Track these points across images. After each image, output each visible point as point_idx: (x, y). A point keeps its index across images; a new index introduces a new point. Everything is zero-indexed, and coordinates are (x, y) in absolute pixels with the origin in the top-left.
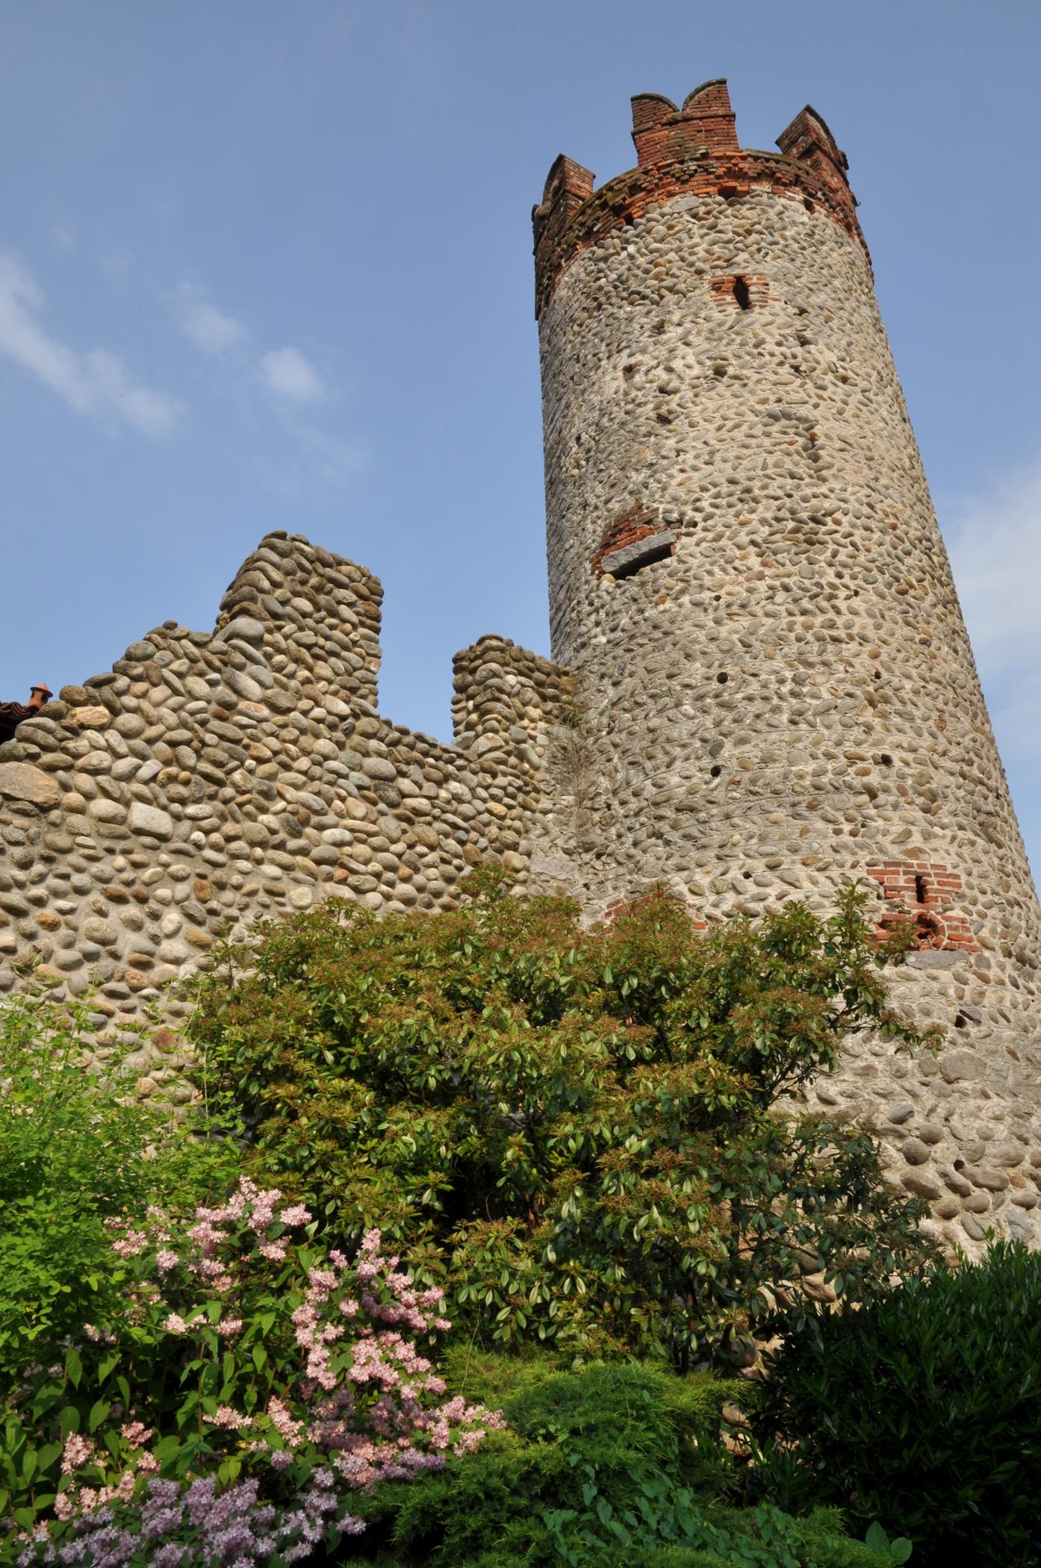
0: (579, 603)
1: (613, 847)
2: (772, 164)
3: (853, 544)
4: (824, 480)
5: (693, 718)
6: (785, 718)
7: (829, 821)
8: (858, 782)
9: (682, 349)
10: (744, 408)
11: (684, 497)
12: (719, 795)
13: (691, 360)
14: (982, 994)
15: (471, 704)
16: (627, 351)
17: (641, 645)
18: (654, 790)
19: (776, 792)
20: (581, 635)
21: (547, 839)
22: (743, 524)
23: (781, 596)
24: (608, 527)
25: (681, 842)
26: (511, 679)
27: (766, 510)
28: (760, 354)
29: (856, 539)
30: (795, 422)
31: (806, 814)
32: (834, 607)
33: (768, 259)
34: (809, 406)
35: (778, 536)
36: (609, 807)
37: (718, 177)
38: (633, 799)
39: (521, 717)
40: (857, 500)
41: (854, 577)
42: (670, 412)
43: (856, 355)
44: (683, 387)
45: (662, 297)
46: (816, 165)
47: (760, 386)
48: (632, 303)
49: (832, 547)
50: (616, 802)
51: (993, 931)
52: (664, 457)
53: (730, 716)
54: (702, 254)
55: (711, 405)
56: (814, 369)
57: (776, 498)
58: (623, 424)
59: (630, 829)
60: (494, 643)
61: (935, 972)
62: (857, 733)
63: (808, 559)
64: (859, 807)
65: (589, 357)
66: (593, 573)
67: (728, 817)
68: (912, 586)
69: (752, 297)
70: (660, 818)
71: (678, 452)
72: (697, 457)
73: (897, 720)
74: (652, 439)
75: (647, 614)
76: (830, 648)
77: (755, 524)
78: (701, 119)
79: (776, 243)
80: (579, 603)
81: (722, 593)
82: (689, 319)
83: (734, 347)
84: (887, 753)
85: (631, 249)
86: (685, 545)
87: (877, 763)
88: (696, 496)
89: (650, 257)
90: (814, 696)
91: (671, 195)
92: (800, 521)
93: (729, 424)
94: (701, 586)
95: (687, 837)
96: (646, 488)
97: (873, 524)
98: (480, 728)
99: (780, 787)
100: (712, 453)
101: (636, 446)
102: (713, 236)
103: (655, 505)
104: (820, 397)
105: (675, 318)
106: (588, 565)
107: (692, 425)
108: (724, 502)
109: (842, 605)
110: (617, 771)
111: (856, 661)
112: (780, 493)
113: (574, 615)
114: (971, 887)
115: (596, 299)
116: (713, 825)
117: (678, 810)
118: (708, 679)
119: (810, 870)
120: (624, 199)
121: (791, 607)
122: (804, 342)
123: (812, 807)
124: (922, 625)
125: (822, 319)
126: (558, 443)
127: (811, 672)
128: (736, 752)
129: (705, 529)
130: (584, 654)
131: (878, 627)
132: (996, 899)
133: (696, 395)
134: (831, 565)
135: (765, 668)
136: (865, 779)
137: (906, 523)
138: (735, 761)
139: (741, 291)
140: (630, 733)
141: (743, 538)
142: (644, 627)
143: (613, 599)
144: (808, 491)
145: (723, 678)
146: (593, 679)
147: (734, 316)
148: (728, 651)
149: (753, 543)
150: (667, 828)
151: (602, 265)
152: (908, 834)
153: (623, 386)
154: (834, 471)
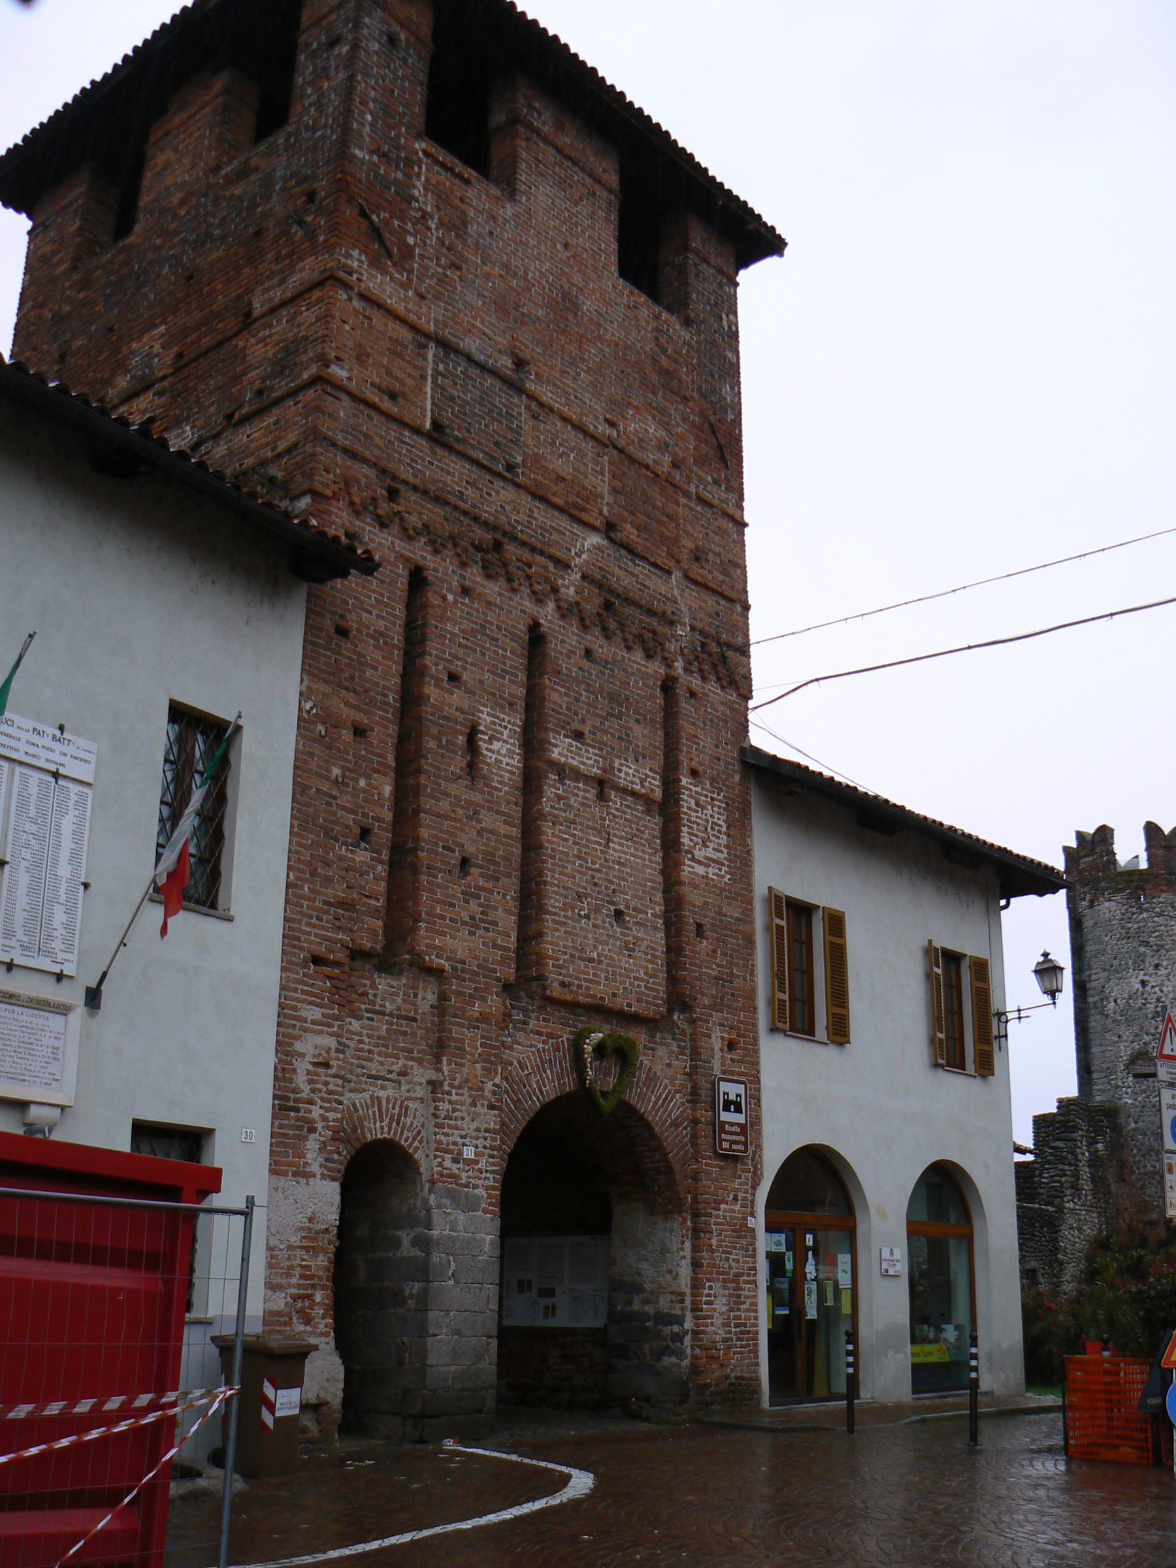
0: (1116, 1079)
9: (1166, 983)
13: (1170, 989)
16: (1142, 972)
91: (1163, 891)
153: (1141, 989)
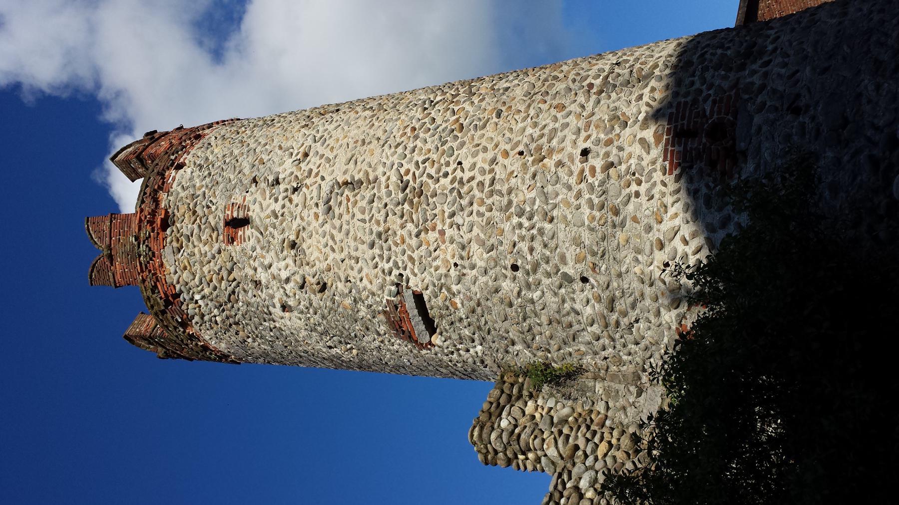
1: (638, 359)
2: (148, 190)
3: (424, 162)
4: (376, 179)
5: (543, 292)
6: (547, 226)
7: (629, 201)
8: (600, 176)
9: (274, 269)
10: (320, 231)
11: (380, 280)
12: (603, 279)
14: (774, 91)
15: (521, 457)
16: (271, 308)
17: (486, 323)
18: (595, 326)
19: (604, 238)
20: (474, 363)
21: (629, 409)
22: (403, 242)
23: (458, 219)
24: (397, 335)
25: (637, 311)
26: (504, 423)
27: (394, 222)
28: (282, 215)
29: (420, 159)
30: (333, 195)
31: (622, 217)
32: (469, 181)
33: (214, 201)
34: (323, 184)
35: (414, 217)
36: (605, 358)
37: (153, 230)
38: (601, 341)
39: (533, 417)
40: (392, 155)
41: (448, 164)
42: (318, 283)
43: (289, 144)
44: (301, 272)
45: (235, 280)
46: (153, 157)
47: (305, 218)
48: (237, 301)
49: (425, 178)
50: (603, 353)
51: (725, 78)
52: (350, 292)
53: (544, 266)
54: (207, 248)
55: (316, 254)
56: (297, 176)
57: (387, 215)
58: (323, 317)
59: (624, 346)
60: (476, 433)
61: (754, 129)
62: (562, 172)
63: (432, 197)
64: (620, 177)
65: (272, 334)
66: (430, 349)
67: (620, 275)
68: (457, 120)
69: (241, 216)
70: (618, 324)
71: (347, 281)
72: (352, 269)
73: (554, 142)
74: (336, 298)
75: (464, 316)
76: (497, 187)
77: (404, 232)
78: (111, 238)
79: (204, 193)
80: (451, 361)
81: (452, 262)
82: (252, 262)
83: (276, 233)
84: (579, 152)
85: (197, 297)
86: (415, 283)
87: (587, 160)
88: (380, 273)
89: (205, 284)
90: (534, 203)
91: (162, 265)
92: (405, 200)
93: (331, 243)
94: (446, 276)
95: (633, 306)
96: (371, 306)
97: (411, 145)
98: (539, 453)
99: (600, 235)
100: (350, 257)
101: (340, 310)
102: (194, 239)
103: (384, 301)
104: (317, 174)
105: (251, 272)
106: (424, 352)
107: (329, 270)
108: (386, 253)
109: (467, 175)
110: (579, 350)
111: (509, 169)
112: (383, 212)
113: (459, 365)
114: (687, 94)
115: (230, 325)
116: (626, 286)
117: (612, 310)
118: (514, 278)
119: (666, 217)
120: (161, 298)
121: (466, 212)
122: (277, 182)
123: (617, 212)
124: (486, 115)
125: (261, 166)
126: (332, 361)
127: (515, 204)
128: (571, 263)
129: (405, 269)
130: (488, 361)
131: (485, 149)
132: (698, 73)
133: (308, 264)
134: (438, 180)
135: (511, 236)
136: (598, 170)
137: (412, 118)
138: (578, 266)
139: (237, 223)
140: (551, 337)
141: (414, 242)
142: (473, 319)
143: (450, 338)
144: (384, 191)
145: (515, 268)
146: (508, 358)
147: (253, 230)
148: (496, 262)
149: (417, 236)
150: (626, 320)
151: (206, 318)
152: (643, 141)
153: (296, 313)
154: (370, 170)
